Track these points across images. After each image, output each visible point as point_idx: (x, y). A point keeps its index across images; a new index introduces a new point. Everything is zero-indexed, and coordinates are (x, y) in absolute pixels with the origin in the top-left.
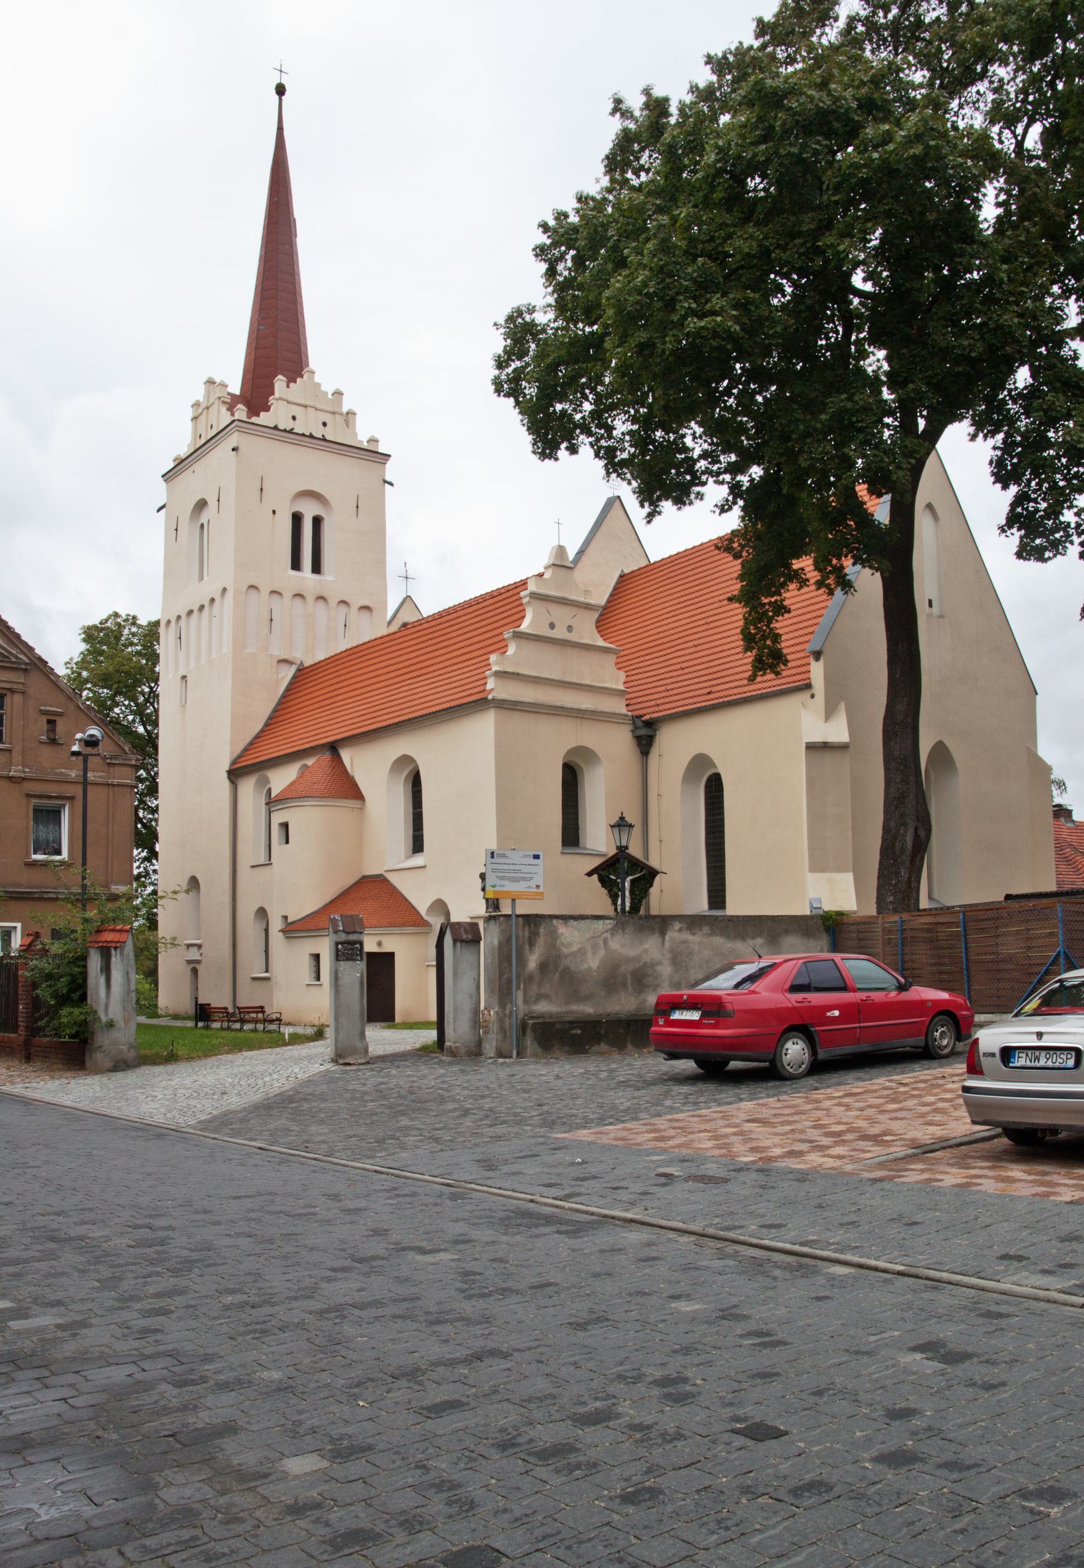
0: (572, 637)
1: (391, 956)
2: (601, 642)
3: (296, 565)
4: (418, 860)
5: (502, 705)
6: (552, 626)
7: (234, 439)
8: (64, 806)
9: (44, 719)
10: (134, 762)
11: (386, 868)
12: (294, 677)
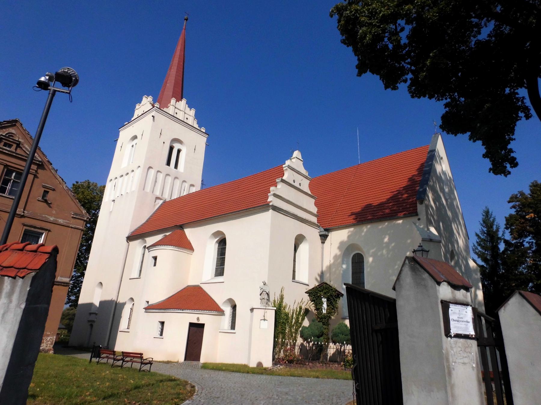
0: (301, 188)
1: (202, 326)
2: (310, 193)
3: (168, 163)
4: (220, 279)
5: (276, 209)
6: (294, 181)
7: (154, 113)
8: (42, 234)
9: (43, 189)
10: (85, 219)
11: (203, 281)
12: (161, 205)
